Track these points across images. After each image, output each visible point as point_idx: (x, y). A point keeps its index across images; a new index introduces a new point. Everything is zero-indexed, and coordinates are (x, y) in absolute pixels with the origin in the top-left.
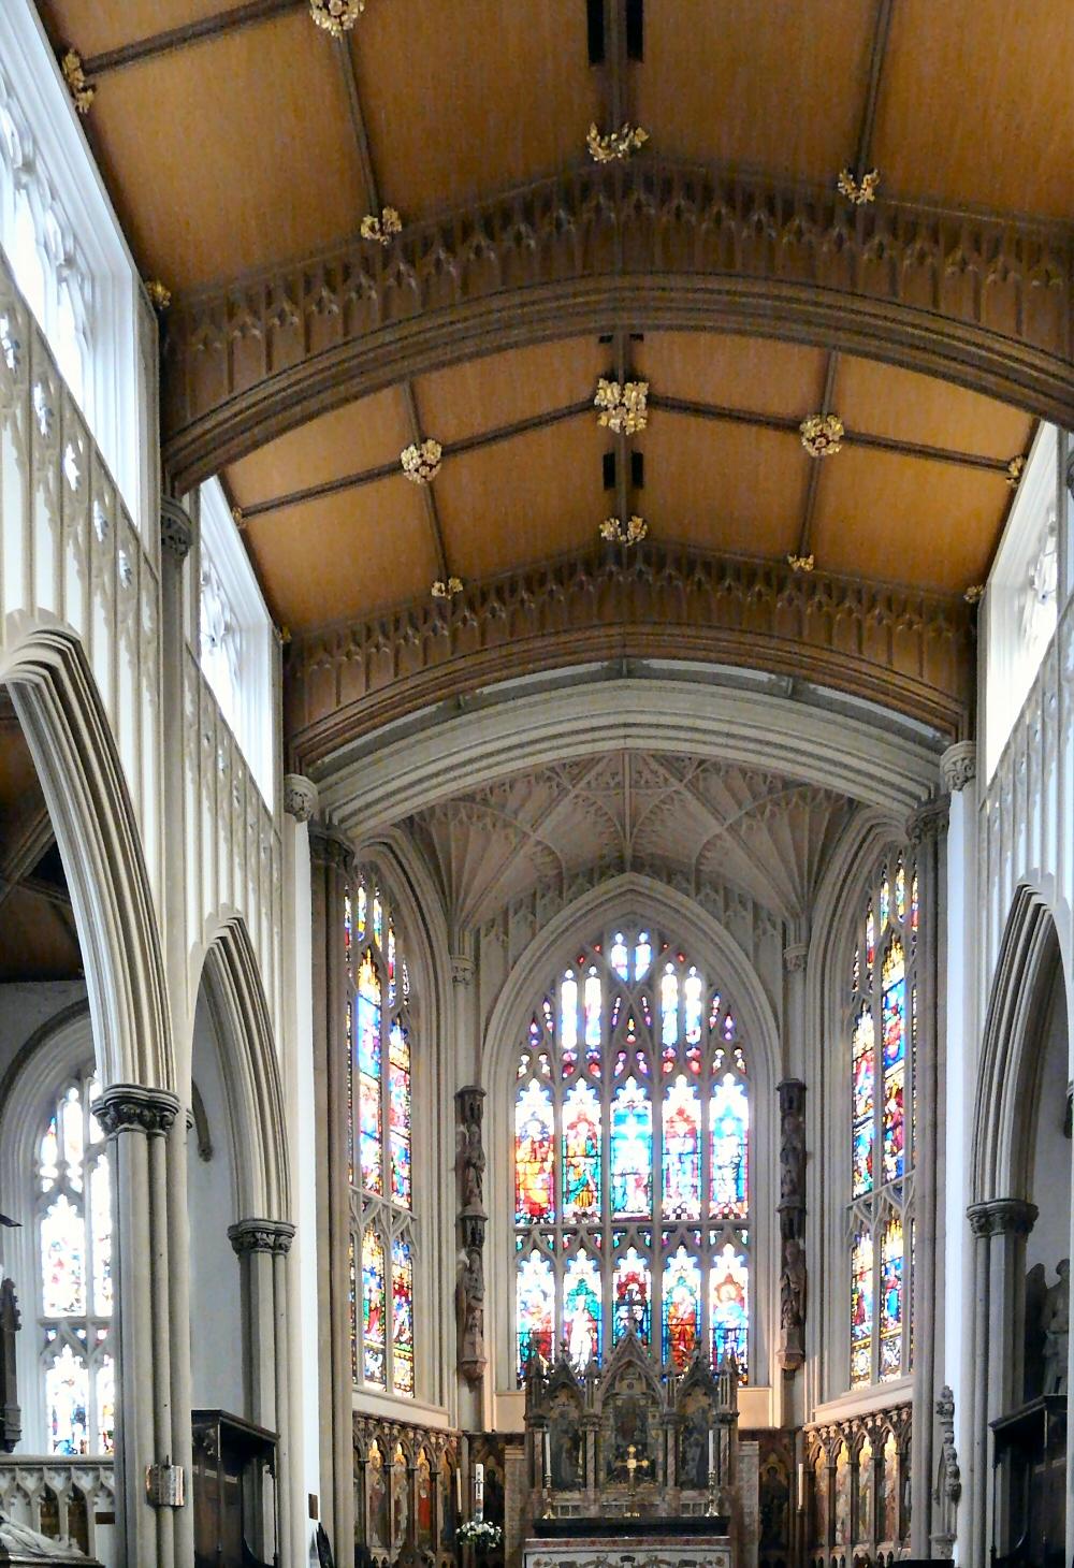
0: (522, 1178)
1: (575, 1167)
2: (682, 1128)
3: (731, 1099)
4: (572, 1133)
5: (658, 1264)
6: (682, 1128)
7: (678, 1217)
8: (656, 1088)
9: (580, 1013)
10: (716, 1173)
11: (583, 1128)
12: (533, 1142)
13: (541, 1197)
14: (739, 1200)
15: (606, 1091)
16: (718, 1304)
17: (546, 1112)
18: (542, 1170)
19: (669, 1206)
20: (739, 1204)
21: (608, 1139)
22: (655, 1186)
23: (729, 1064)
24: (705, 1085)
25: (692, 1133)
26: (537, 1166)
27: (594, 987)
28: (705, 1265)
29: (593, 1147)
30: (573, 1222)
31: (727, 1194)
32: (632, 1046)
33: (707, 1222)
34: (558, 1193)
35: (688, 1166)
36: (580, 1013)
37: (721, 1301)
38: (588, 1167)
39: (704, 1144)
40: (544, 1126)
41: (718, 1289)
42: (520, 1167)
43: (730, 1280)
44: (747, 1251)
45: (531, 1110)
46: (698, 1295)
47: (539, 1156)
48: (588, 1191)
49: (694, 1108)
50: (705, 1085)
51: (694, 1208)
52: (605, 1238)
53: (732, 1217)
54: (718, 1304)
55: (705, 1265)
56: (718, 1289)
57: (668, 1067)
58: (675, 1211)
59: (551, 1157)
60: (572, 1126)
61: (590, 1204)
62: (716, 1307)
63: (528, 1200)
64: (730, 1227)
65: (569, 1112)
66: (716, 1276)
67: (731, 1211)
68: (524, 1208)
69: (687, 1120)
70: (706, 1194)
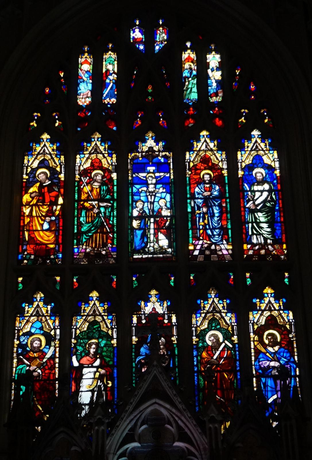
0: (27, 220)
1: (88, 210)
2: (206, 174)
3: (261, 155)
4: (85, 180)
5: (185, 304)
6: (206, 174)
7: (207, 258)
8: (179, 142)
9: (93, 78)
10: (249, 217)
11: (98, 173)
12: (41, 187)
13: (46, 237)
14: (276, 241)
15: (122, 144)
16: (259, 347)
17: (58, 162)
18: (50, 213)
19: (195, 247)
20: (276, 246)
21: (125, 185)
22: (179, 226)
23: (255, 122)
24: (231, 142)
25: (218, 179)
26: (45, 209)
27: (110, 63)
28: (242, 307)
29: (110, 191)
30: (84, 262)
31: (261, 231)
32: (150, 104)
33: (239, 261)
34: (65, 227)
35: (216, 211)
36: (93, 78)
37: (265, 346)
38: (102, 210)
39: (234, 188)
40: (53, 170)
41: (259, 332)
42: (27, 211)
43: (271, 322)
44: (288, 296)
45: (42, 156)
46: (235, 338)
47: (47, 199)
48: (102, 232)
49: (219, 158)
50: (231, 142)
51: (225, 248)
52: (121, 276)
53: (270, 258)
54: (259, 347)
55: (242, 307)
56: (259, 332)
57: (191, 123)
58: (202, 251)
59: (61, 201)
60: (86, 173)
61: (105, 245)
62: (258, 352)
63: (33, 240)
64: (265, 270)
65: (83, 162)
66: (257, 318)
67: (268, 251)
68: (30, 248)
69: (214, 167)
70: (239, 236)
